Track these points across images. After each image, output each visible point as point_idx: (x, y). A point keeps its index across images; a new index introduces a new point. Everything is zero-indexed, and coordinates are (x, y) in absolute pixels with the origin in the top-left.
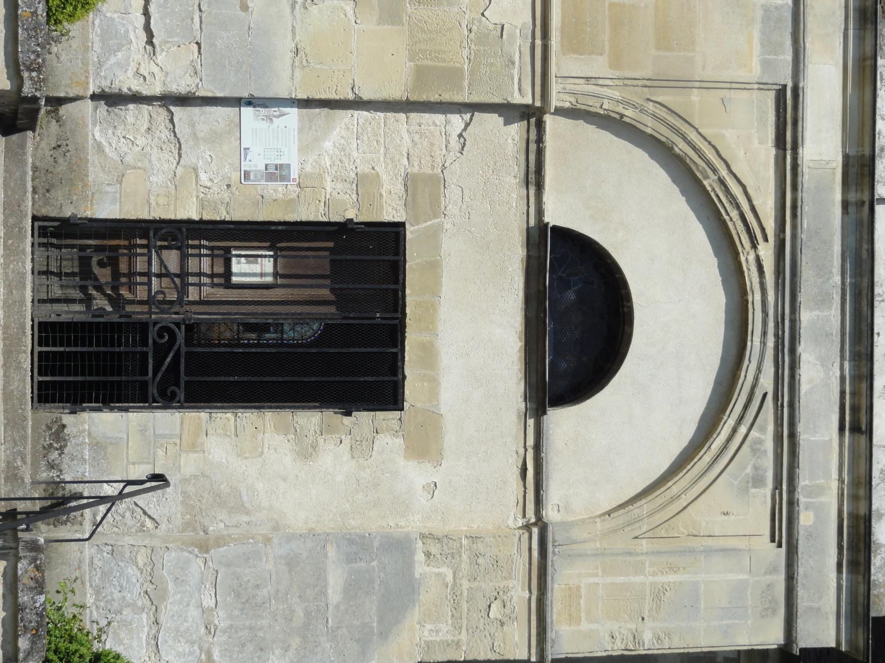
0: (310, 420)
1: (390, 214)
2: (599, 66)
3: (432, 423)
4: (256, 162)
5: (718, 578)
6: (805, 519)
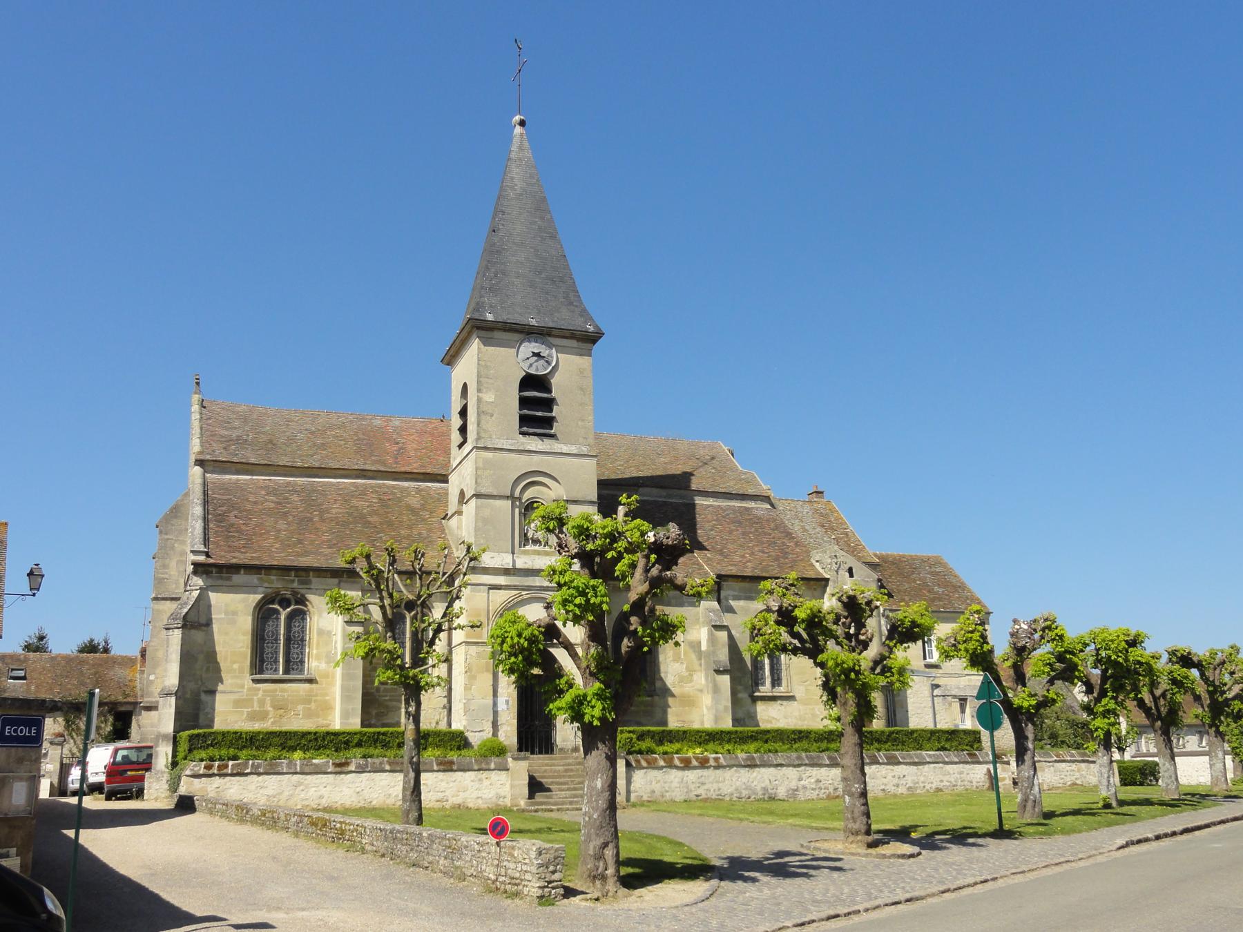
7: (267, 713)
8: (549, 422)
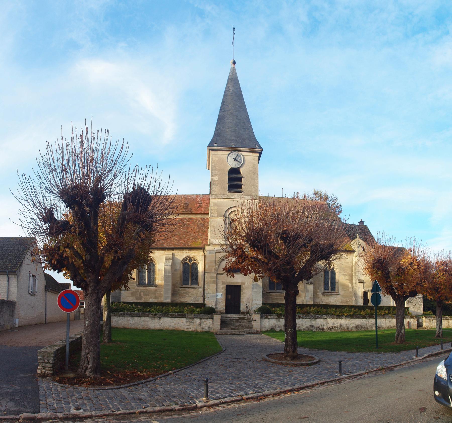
0: (242, 293)
1: (225, 286)
2: (213, 268)
3: (242, 283)
4: (221, 296)
8: (240, 186)
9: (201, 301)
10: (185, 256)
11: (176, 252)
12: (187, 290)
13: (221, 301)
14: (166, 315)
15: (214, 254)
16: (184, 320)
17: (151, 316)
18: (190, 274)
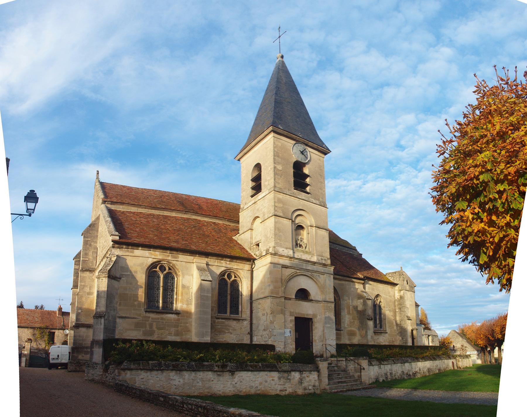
3: (314, 315)
5: (328, 281)
6: (322, 271)
7: (154, 332)
9: (246, 340)
10: (223, 269)
11: (212, 261)
12: (227, 322)
13: (289, 341)
14: (243, 367)
15: (280, 270)
16: (275, 375)
17: (216, 369)
18: (229, 297)
